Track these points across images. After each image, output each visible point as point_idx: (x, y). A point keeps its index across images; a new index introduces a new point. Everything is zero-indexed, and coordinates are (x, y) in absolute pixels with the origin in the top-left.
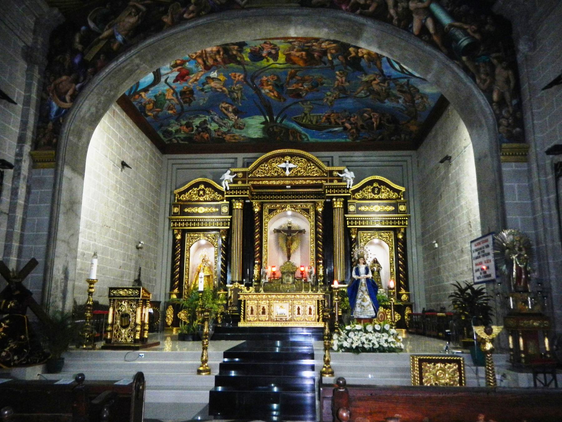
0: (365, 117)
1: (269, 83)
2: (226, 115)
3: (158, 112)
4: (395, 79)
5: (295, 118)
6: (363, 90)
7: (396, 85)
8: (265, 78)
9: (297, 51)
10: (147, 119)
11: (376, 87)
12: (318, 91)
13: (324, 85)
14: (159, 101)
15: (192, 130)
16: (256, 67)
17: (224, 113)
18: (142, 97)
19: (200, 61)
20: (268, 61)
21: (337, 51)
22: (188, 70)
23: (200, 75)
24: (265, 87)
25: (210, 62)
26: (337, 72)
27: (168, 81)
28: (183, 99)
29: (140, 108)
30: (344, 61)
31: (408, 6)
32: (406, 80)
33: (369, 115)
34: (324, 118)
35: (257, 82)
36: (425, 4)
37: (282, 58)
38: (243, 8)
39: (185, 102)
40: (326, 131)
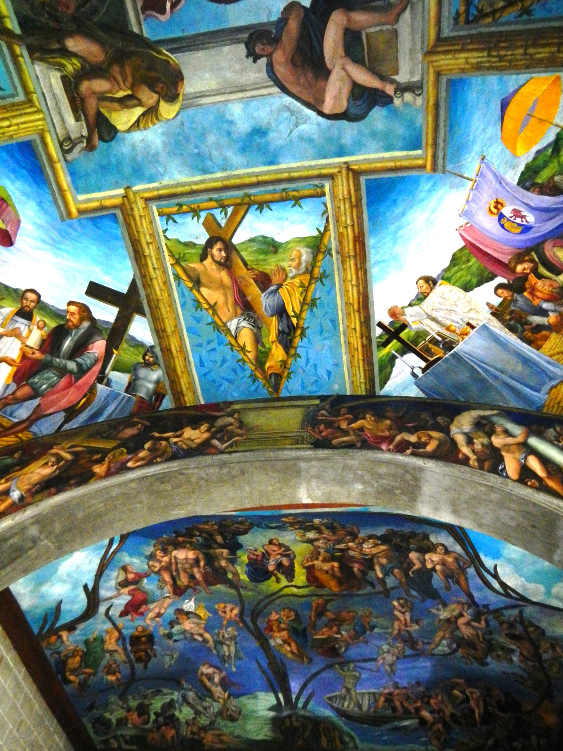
0: (457, 697)
1: (283, 626)
2: (209, 691)
3: (90, 675)
4: (496, 611)
5: (330, 699)
6: (443, 638)
7: (501, 623)
8: (274, 616)
9: (325, 561)
10: (68, 688)
11: (466, 632)
12: (366, 642)
13: (376, 630)
14: (91, 652)
15: (147, 722)
16: (259, 593)
17: (205, 686)
18: (63, 642)
19: (167, 577)
20: (278, 581)
21: (390, 562)
22: (146, 593)
23: (165, 605)
24: (276, 634)
25: (184, 580)
26: (395, 603)
27: (111, 613)
28: (135, 653)
29: (57, 663)
30: (404, 580)
31: (491, 443)
32: (516, 612)
33: (463, 692)
34: (382, 699)
35: (262, 623)
36: (520, 439)
37: (300, 577)
38: (222, 452)
39: (139, 660)
40: (388, 726)
